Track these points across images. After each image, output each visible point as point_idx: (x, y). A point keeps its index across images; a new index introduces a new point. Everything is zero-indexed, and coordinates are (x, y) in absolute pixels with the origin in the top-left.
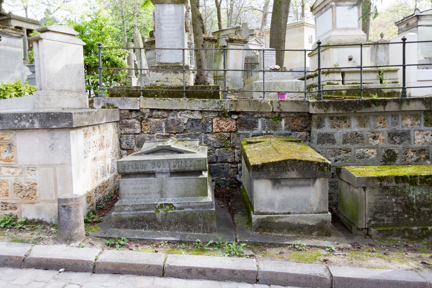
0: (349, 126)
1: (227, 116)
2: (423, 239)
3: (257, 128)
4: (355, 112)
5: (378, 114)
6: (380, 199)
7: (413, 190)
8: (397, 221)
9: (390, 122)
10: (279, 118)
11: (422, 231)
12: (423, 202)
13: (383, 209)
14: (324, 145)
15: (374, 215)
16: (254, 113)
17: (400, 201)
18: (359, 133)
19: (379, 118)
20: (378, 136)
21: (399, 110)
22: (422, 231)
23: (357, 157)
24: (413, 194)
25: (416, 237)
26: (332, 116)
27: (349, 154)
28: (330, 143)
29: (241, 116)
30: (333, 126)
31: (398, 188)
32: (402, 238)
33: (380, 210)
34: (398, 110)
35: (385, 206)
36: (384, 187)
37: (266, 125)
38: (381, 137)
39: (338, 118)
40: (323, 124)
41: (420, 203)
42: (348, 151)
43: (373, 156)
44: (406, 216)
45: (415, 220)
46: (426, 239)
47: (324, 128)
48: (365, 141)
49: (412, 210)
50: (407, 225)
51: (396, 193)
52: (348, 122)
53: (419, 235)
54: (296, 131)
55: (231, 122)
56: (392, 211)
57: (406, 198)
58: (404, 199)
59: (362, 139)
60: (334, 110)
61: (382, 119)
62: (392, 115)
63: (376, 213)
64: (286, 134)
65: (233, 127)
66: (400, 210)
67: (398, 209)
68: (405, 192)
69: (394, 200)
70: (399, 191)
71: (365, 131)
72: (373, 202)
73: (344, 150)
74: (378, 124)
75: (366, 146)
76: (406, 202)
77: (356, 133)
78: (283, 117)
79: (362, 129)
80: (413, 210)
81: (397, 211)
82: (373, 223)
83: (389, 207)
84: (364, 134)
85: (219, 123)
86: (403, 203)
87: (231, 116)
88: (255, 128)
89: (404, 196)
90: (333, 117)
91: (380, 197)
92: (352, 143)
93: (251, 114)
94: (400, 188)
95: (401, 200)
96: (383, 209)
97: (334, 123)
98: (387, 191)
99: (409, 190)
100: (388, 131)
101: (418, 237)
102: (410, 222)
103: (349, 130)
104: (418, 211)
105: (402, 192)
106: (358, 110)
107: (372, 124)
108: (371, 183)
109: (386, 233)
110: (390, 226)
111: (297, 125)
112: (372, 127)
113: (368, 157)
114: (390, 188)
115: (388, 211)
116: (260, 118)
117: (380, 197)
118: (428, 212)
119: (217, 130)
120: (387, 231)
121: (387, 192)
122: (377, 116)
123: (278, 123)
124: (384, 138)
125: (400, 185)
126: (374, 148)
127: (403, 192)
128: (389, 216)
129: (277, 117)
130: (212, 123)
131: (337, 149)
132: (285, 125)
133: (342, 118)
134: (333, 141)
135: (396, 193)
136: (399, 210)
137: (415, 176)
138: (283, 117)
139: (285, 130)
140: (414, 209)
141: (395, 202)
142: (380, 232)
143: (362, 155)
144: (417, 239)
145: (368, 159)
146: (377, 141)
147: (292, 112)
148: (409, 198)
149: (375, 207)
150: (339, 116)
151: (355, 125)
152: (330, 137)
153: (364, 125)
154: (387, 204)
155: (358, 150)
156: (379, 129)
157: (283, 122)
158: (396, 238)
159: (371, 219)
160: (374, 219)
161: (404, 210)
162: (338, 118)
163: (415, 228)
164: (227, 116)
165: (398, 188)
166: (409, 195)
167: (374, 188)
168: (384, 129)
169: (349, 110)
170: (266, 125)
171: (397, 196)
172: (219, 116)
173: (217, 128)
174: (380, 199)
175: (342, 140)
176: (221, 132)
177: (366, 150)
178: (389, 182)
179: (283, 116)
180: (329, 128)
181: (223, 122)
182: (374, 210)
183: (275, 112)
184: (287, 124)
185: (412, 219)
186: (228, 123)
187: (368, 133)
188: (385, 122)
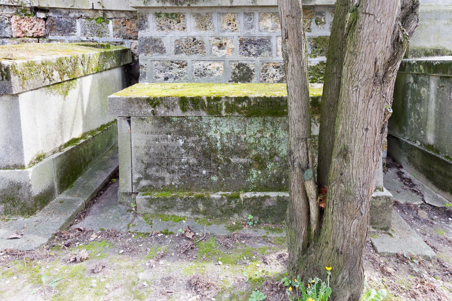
0: (184, 28)
1: (30, 13)
3: (75, 32)
4: (189, 5)
5: (224, 11)
6: (157, 140)
7: (216, 123)
9: (242, 23)
10: (105, 20)
12: (235, 146)
13: (162, 159)
14: (149, 55)
15: (146, 168)
16: (70, 10)
17: (194, 145)
18: (198, 38)
19: (227, 17)
20: (225, 43)
21: (254, 4)
22: (229, 202)
23: (195, 73)
24: (216, 132)
26: (158, 12)
27: (184, 70)
28: (156, 51)
29: (50, 14)
30: (161, 27)
31: (189, 121)
32: (193, 213)
33: (159, 160)
34: (251, 4)
35: (164, 152)
36: (163, 117)
37: (88, 29)
38: (230, 45)
39: (167, 15)
40: (146, 23)
41: (228, 148)
42: (183, 65)
43: (218, 74)
44: (204, 172)
45: (220, 179)
47: (147, 30)
48: (207, 51)
49: (214, 161)
50: (207, 189)
51: (185, 130)
52: (182, 22)
54: (130, 38)
55: (35, 22)
56: (178, 162)
57: (204, 138)
58: (200, 140)
59: (202, 47)
60: (158, 2)
61: (232, 19)
62: (245, 14)
63: (149, 166)
64: (116, 42)
65: (41, 30)
66: (193, 161)
67: (188, 160)
68: (202, 128)
69: (181, 142)
70: (190, 125)
71: (206, 36)
72: (144, 145)
73: (178, 64)
74: (225, 26)
75: (208, 58)
76: (203, 146)
77: (194, 39)
78: (111, 19)
79: (203, 32)
80: (216, 161)
81: (187, 163)
83: (173, 155)
84: (206, 40)
85: (20, 24)
86: (199, 149)
87: (35, 14)
88: (72, 33)
89: (199, 136)
90: (160, 13)
91: (156, 136)
92: (188, 53)
93: (64, 11)
94: (192, 121)
95: (193, 142)
96: (162, 159)
97: (163, 22)
98: (169, 125)
99: (209, 124)
100: (239, 37)
102: (212, 182)
103: (184, 34)
104: (226, 163)
105: (194, 127)
106: (193, 3)
107: (216, 26)
111: (130, 30)
112: (216, 30)
113: (211, 75)
114: (172, 121)
115: (172, 162)
116: (78, 18)
117: (156, 136)
118: (243, 165)
119: (19, 34)
121: (167, 127)
122: (224, 14)
123: (104, 27)
124: (233, 46)
125: (190, 114)
126: (218, 61)
127: (198, 128)
128: (173, 172)
129: (101, 18)
130: (10, 24)
131: (167, 61)
132: (114, 29)
133: (174, 16)
134: (162, 50)
135: (185, 130)
136: (191, 161)
137: (218, 99)
138: (111, 19)
139: (114, 36)
140: (218, 159)
141: (184, 146)
142: (151, 201)
143: (202, 70)
145: (212, 77)
146: (223, 51)
147: (123, 11)
148: (208, 138)
149: (147, 154)
150: (169, 11)
151: (192, 26)
152: (156, 44)
153: (206, 26)
154: (169, 149)
155: (197, 64)
156: (226, 34)
157: (111, 25)
161: (200, 161)
162: (167, 15)
164: (30, 13)
165: (189, 121)
166: (209, 134)
167: (143, 120)
168: (234, 33)
169: (180, 3)
170: (88, 29)
171: (188, 134)
172: (17, 13)
173: (17, 31)
174: (157, 140)
175: (173, 49)
176: (24, 37)
177: (209, 63)
179: (110, 17)
180: (155, 30)
181: (25, 23)
182: (146, 159)
183: (97, 10)
184: (117, 28)
185: (215, 178)
186: (32, 24)
187: (210, 39)
188: (235, 23)
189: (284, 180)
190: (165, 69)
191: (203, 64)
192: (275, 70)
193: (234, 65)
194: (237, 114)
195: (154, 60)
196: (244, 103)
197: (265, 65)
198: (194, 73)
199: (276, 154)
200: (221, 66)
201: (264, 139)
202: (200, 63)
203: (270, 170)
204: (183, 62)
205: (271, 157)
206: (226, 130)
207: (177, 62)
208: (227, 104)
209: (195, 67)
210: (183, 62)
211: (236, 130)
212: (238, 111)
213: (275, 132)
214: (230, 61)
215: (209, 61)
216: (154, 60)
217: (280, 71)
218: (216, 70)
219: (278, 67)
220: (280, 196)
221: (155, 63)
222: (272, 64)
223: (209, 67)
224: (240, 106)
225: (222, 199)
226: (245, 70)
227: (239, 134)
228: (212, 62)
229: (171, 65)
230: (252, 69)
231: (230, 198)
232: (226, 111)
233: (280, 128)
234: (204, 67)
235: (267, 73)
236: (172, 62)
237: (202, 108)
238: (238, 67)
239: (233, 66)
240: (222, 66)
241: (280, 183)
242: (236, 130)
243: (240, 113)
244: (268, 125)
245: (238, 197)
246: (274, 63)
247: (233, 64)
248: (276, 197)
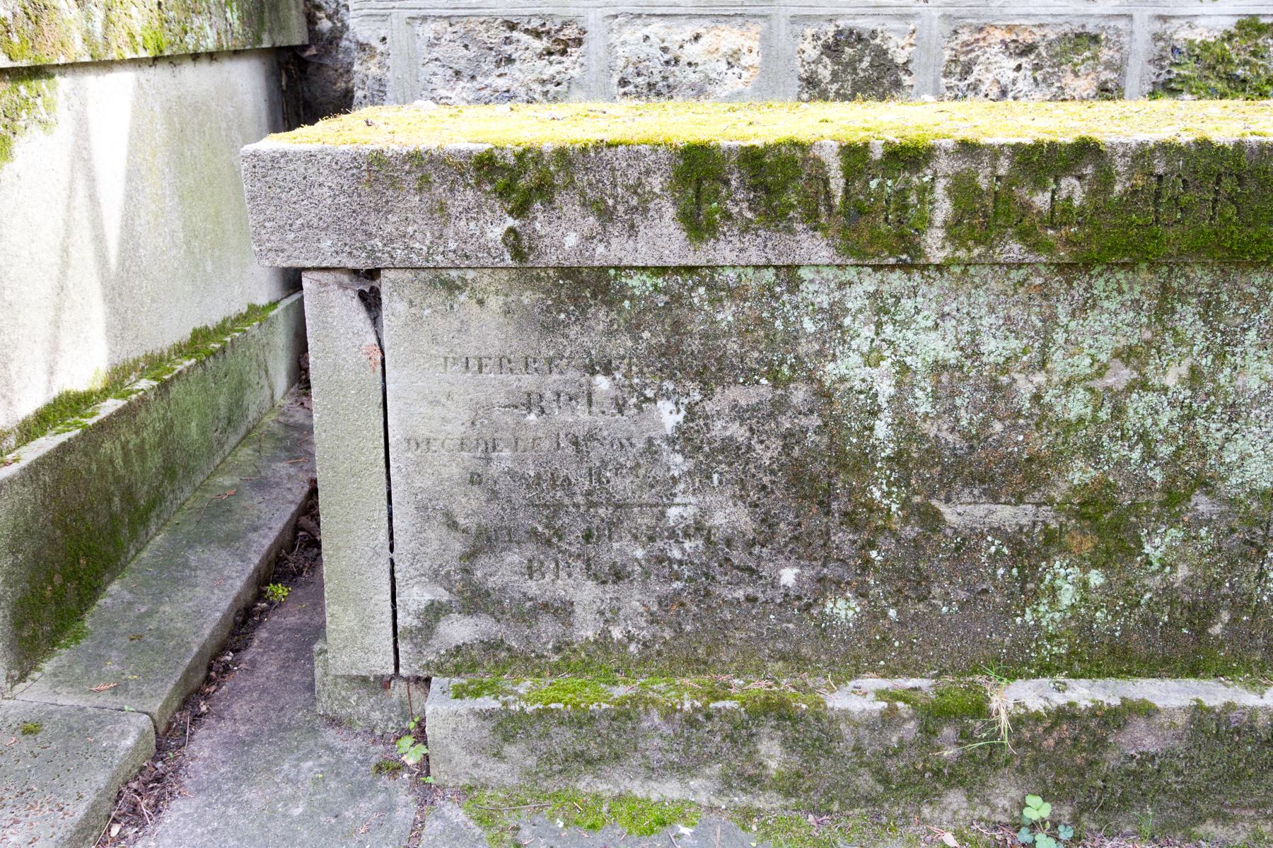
2: (927, 796)
6: (531, 402)
8: (698, 625)
11: (928, 732)
13: (558, 507)
15: (471, 555)
17: (738, 432)
23: (623, 82)
24: (872, 359)
25: (865, 782)
27: (569, 65)
35: (570, 470)
36: (568, 272)
41: (934, 451)
44: (788, 576)
46: (955, 799)
49: (849, 519)
53: (892, 765)
56: (645, 521)
58: (780, 405)
63: (484, 542)
66: (729, 515)
67: (705, 511)
68: (793, 338)
69: (668, 416)
70: (726, 316)
72: (457, 430)
73: (537, 35)
76: (790, 438)
81: (698, 528)
82: (459, 630)
83: (622, 486)
86: (767, 453)
89: (776, 381)
91: (528, 381)
95: (739, 413)
98: (601, 317)
99: (834, 315)
101: (885, 780)
102: (824, 629)
104: (910, 532)
108: (406, 230)
109: (564, 738)
110: (627, 668)
115: (613, 525)
117: (528, 381)
118: (1008, 539)
120: (582, 721)
121: (595, 330)
125: (729, 252)
128: (619, 575)
131: (488, 22)
135: (695, 345)
136: (719, 519)
140: (871, 507)
141: (685, 439)
144: (870, 800)
148: (826, 395)
149: (475, 479)
154: (596, 453)
155: (632, 34)
158: (670, 789)
159: (444, 596)
160: (476, 600)
161: (768, 522)
163: (857, 699)
174: (531, 402)
178: (606, 215)
182: (470, 507)
185: (844, 609)
189: (1225, 616)
191: (662, 33)
192: (1013, 63)
193: (816, 37)
194: (1014, 249)
195: (424, 19)
196: (1070, 185)
197: (965, 36)
198: (616, 80)
199: (1204, 484)
200: (748, 44)
201: (1151, 397)
202: (646, 31)
203: (1156, 565)
204: (565, 24)
205: (1173, 498)
206: (937, 346)
207: (535, 23)
208: (962, 188)
209: (620, 50)
210: (565, 24)
211: (994, 347)
212: (1023, 235)
213: (1220, 357)
214: (794, 19)
215: (690, 16)
216: (424, 19)
217: (1037, 67)
218: (723, 66)
219: (1028, 49)
220: (1209, 702)
221: (428, 30)
222: (998, 35)
223: (692, 52)
224: (1041, 200)
225: (889, 719)
226: (865, 64)
227: (1004, 368)
228: (707, 22)
229: (508, 41)
230: (900, 60)
231: (934, 716)
232: (954, 232)
233: (1252, 335)
234: (665, 50)
235: (971, 79)
236: (512, 27)
237: (811, 216)
238: (832, 50)
240: (756, 46)
241: (1200, 633)
242: (994, 347)
243: (1035, 247)
244: (1188, 318)
245: (980, 710)
246: (1010, 29)
247: (809, 32)
248: (1184, 710)
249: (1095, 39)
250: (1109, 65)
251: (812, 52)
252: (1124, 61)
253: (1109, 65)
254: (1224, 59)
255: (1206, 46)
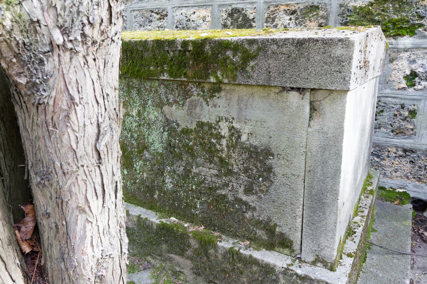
23: (177, 27)
27: (163, 23)
73: (157, 14)
155: (178, 12)
190: (144, 22)
191: (185, 12)
192: (288, 17)
193: (226, 11)
195: (134, 10)
197: (272, 9)
198: (175, 26)
200: (207, 14)
202: (181, 11)
204: (163, 10)
207: (157, 10)
209: (176, 18)
210: (163, 10)
213: (144, 108)
214: (220, 6)
215: (193, 6)
216: (134, 10)
217: (297, 19)
218: (201, 21)
219: (293, 12)
222: (283, 8)
223: (193, 17)
226: (240, 19)
228: (196, 8)
229: (151, 16)
230: (251, 18)
234: (186, 17)
235: (274, 24)
236: (152, 12)
238: (231, 15)
239: (223, 14)
240: (209, 14)
244: (134, 93)
246: (287, 5)
247: (224, 10)
249: (317, 7)
250: (322, 17)
251: (225, 16)
252: (328, 15)
253: (322, 17)
254: (369, 13)
255: (361, 8)
